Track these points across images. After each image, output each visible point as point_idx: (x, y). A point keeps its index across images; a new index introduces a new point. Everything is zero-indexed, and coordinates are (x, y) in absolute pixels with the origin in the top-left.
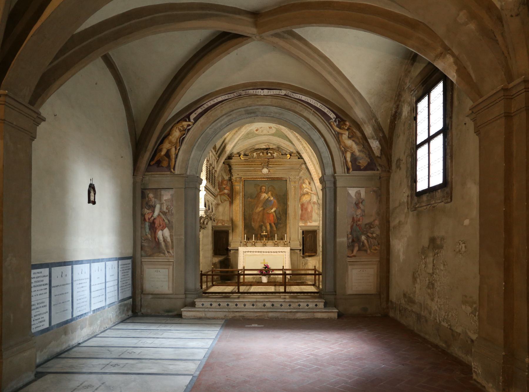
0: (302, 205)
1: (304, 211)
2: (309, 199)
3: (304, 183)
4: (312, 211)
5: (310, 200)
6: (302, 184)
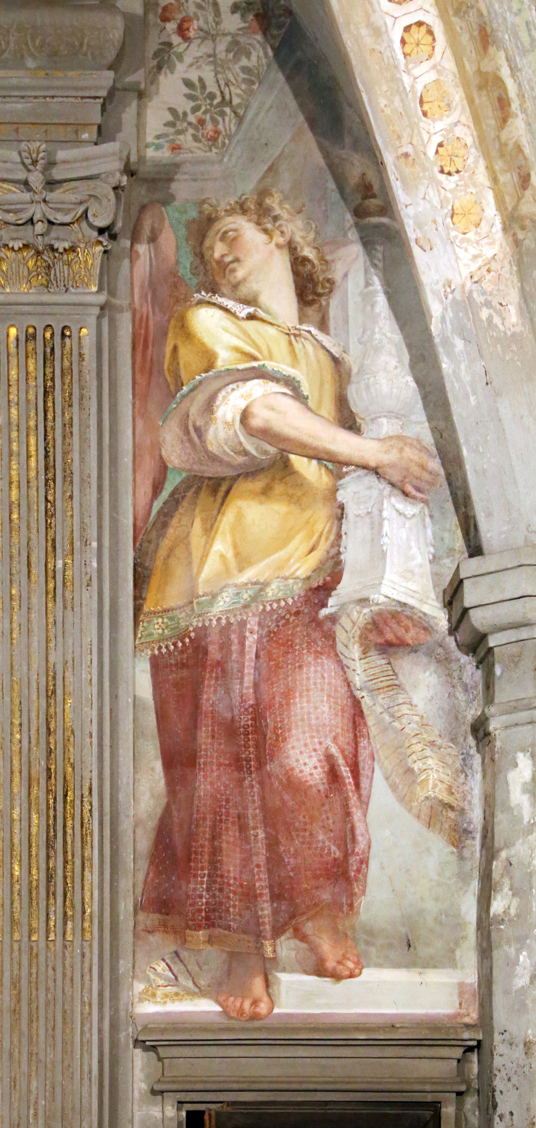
0: (188, 667)
1: (210, 781)
2: (299, 564)
3: (213, 279)
4: (345, 775)
5: (321, 590)
6: (172, 297)
